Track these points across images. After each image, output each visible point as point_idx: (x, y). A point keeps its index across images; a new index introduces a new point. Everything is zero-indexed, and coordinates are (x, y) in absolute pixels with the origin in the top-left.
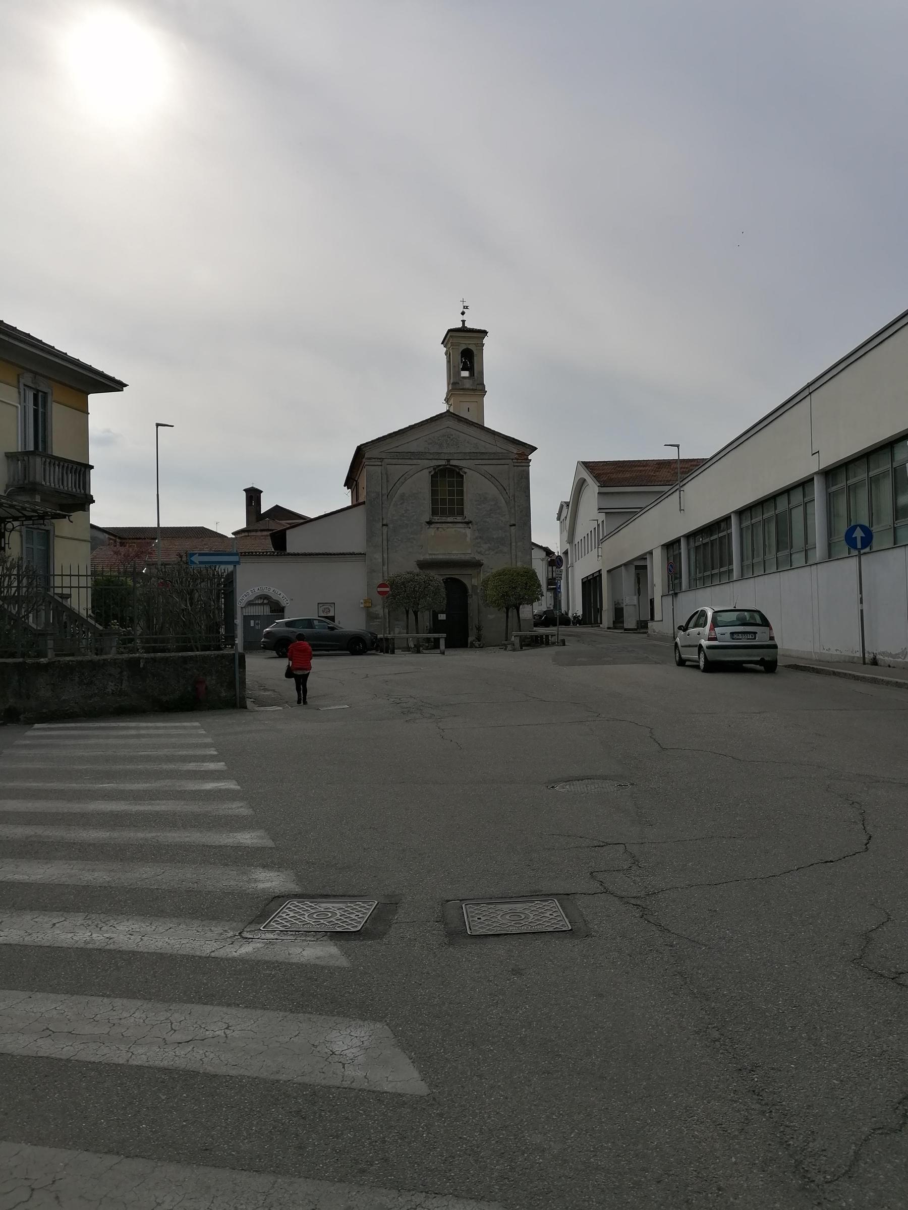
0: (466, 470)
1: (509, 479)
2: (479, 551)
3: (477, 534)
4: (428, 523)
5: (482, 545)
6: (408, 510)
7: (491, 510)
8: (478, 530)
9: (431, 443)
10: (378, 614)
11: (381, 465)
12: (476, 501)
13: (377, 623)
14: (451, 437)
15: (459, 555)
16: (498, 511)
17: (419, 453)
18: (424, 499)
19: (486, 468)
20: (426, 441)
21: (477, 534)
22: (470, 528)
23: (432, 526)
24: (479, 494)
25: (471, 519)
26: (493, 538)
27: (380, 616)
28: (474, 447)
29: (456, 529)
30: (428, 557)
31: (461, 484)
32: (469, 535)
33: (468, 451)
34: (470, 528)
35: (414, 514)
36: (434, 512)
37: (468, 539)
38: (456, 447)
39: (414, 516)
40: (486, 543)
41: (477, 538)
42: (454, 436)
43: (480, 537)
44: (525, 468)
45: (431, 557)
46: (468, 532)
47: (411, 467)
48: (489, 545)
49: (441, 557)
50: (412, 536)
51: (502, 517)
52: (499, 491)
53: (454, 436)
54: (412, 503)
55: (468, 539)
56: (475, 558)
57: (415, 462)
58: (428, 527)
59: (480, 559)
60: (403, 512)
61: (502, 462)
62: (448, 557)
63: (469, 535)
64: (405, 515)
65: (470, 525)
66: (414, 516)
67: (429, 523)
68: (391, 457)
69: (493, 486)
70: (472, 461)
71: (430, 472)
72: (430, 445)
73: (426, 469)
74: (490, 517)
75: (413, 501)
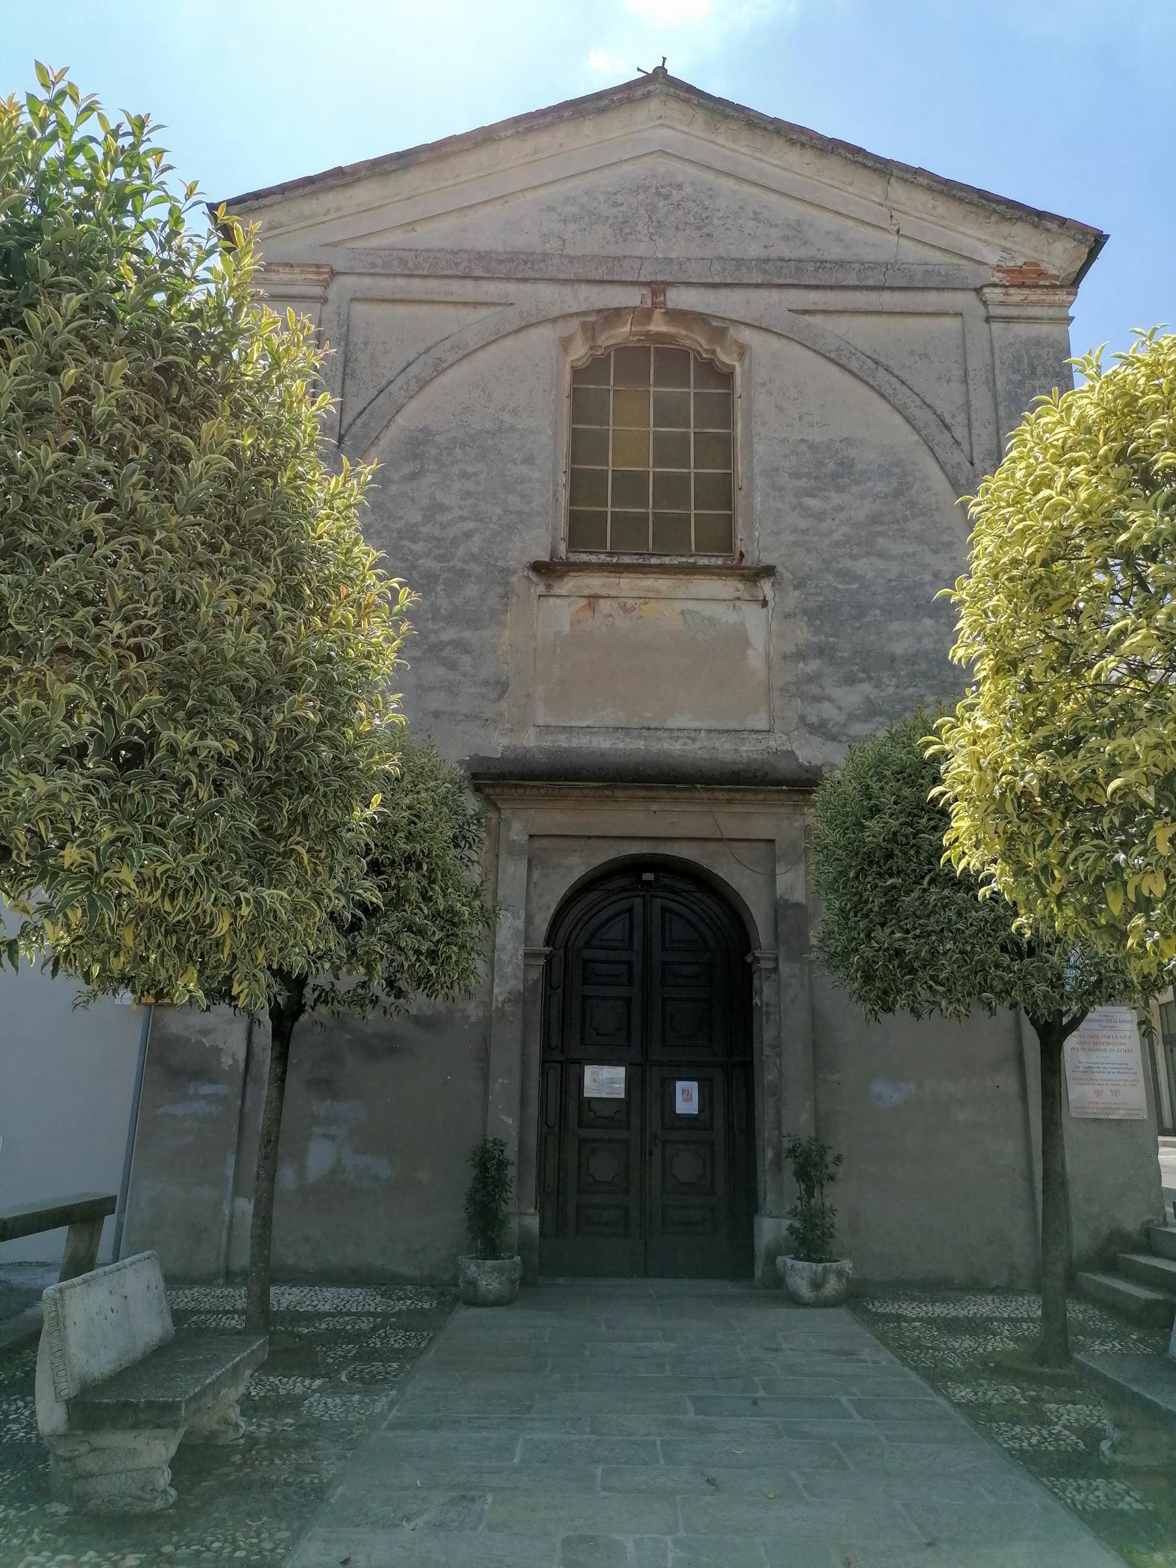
0: (746, 335)
1: (965, 379)
2: (813, 719)
3: (803, 634)
4: (538, 568)
5: (830, 691)
6: (443, 508)
7: (875, 519)
8: (806, 612)
9: (576, 219)
10: (216, 1051)
11: (324, 300)
12: (796, 475)
13: (202, 1108)
14: (676, 196)
15: (703, 740)
16: (914, 526)
17: (515, 257)
18: (529, 460)
19: (843, 325)
20: (551, 209)
21: (803, 634)
22: (765, 603)
23: (568, 585)
24: (813, 447)
25: (767, 559)
26: (893, 658)
27: (227, 1062)
28: (786, 238)
29: (691, 605)
30: (530, 741)
31: (723, 410)
32: (757, 638)
33: (754, 250)
34: (765, 603)
35: (470, 525)
36: (575, 540)
37: (755, 660)
38: (696, 234)
39: (468, 535)
40: (851, 680)
41: (801, 655)
42: (688, 190)
43: (821, 651)
44: (1044, 329)
45: (547, 742)
46: (753, 619)
47: (471, 315)
48: (867, 688)
49: (603, 743)
50: (449, 634)
51: (935, 552)
52: (918, 432)
53: (688, 190)
54: (465, 476)
55: (755, 660)
56: (791, 753)
57: (492, 289)
58: (541, 589)
59: (817, 762)
60: (419, 518)
61: (932, 300)
62: (641, 744)
63: (757, 638)
64: (424, 530)
65: (766, 587)
66: (468, 535)
67: (547, 570)
68: (373, 265)
69: (883, 406)
70: (775, 294)
71: (565, 343)
72: (572, 226)
73: (549, 326)
74: (868, 554)
75: (470, 469)
